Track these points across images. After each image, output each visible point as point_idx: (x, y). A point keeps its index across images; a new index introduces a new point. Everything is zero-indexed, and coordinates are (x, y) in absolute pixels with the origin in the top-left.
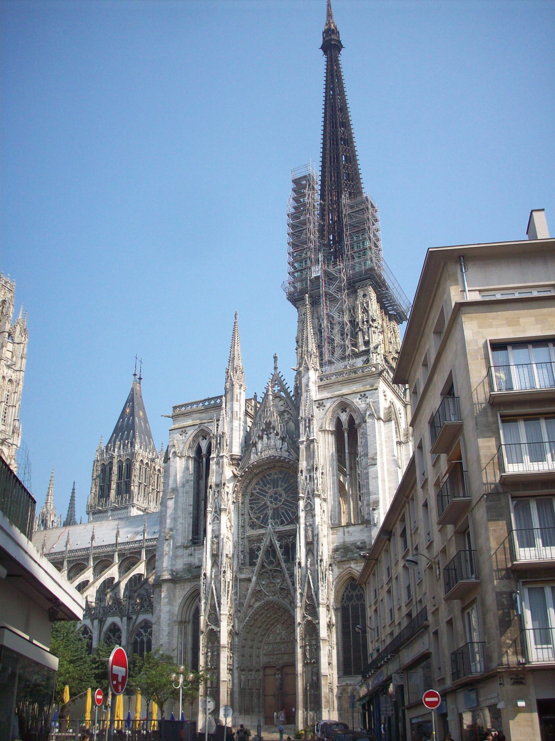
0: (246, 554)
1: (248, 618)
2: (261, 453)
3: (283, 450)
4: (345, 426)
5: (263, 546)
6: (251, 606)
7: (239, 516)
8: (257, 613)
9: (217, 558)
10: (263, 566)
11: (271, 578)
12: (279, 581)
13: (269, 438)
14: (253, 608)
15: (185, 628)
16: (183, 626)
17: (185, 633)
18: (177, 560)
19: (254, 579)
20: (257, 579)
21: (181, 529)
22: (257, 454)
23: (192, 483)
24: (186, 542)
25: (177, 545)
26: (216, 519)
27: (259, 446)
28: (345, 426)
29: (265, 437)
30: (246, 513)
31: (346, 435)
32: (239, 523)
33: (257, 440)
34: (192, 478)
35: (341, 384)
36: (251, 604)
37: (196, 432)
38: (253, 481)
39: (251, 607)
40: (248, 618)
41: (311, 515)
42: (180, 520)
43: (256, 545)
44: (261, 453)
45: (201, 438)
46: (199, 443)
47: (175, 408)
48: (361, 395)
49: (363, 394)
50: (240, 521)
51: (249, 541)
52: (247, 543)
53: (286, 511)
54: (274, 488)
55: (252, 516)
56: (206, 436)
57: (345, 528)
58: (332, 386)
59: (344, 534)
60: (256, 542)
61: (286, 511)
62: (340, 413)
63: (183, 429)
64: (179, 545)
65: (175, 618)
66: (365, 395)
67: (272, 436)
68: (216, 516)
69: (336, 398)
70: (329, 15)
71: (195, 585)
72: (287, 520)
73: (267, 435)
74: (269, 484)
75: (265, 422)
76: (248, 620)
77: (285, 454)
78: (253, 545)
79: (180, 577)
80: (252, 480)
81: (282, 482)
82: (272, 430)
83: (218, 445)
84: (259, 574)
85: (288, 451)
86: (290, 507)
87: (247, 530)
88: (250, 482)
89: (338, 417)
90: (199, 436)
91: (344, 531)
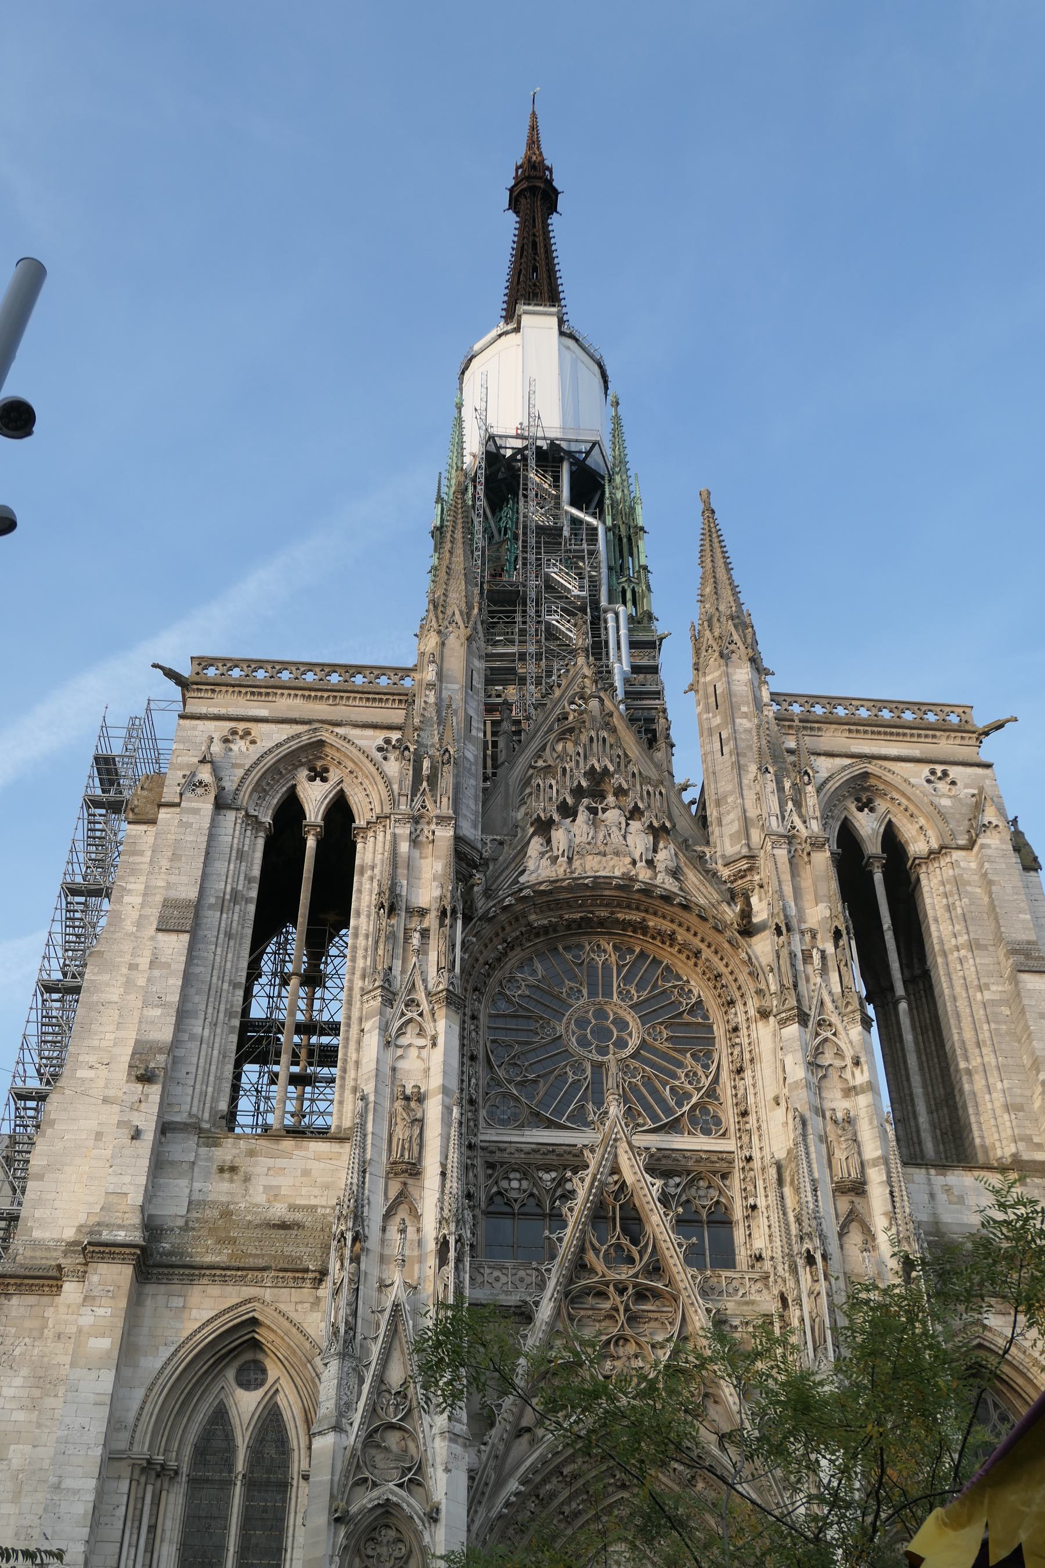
0: (477, 1212)
1: (513, 1485)
2: (570, 860)
3: (660, 867)
4: (873, 847)
5: (582, 1188)
6: (528, 1430)
7: (463, 1055)
8: (558, 1471)
9: (410, 1181)
10: (580, 1266)
11: (622, 1318)
12: (659, 1338)
13: (595, 824)
14: (532, 1443)
15: (156, 1502)
16: (150, 1488)
17: (152, 1528)
18: (162, 1181)
19: (545, 1312)
20: (557, 1314)
21: (194, 1060)
22: (554, 860)
23: (252, 908)
24: (206, 1116)
25: (168, 1118)
26: (411, 1029)
27: (559, 836)
28: (873, 847)
29: (582, 816)
30: (481, 1056)
31: (878, 877)
32: (462, 1081)
33: (556, 817)
34: (254, 894)
35: (850, 731)
36: (524, 1423)
37: (294, 745)
38: (511, 954)
39: (526, 1437)
40: (513, 1485)
41: (840, 1085)
42: (197, 1027)
43: (515, 1184)
44: (570, 860)
45: (303, 773)
46: (294, 787)
47: (203, 662)
48: (933, 772)
49: (939, 768)
50: (466, 1078)
51: (491, 1165)
52: (480, 1170)
53: (647, 1082)
54: (591, 994)
55: (501, 1073)
56: (327, 770)
57: (932, 1171)
58: (819, 729)
59: (932, 1196)
60: (518, 1175)
61: (647, 1082)
62: (853, 807)
63: (241, 726)
64: (177, 1119)
65: (121, 1442)
66: (945, 774)
67: (613, 816)
68: (411, 1020)
69: (848, 761)
70: (533, 142)
71: (249, 1301)
72: (655, 1118)
73: (593, 811)
74: (574, 978)
75: (588, 768)
76: (517, 1494)
77: (670, 884)
78: (504, 1184)
79: (170, 1254)
80: (512, 949)
81: (627, 980)
82: (611, 799)
83: (425, 784)
84: (567, 1294)
85: (675, 873)
86: (662, 1070)
87: (482, 1123)
88: (506, 954)
89: (846, 818)
90: (302, 765)
91: (929, 1182)
